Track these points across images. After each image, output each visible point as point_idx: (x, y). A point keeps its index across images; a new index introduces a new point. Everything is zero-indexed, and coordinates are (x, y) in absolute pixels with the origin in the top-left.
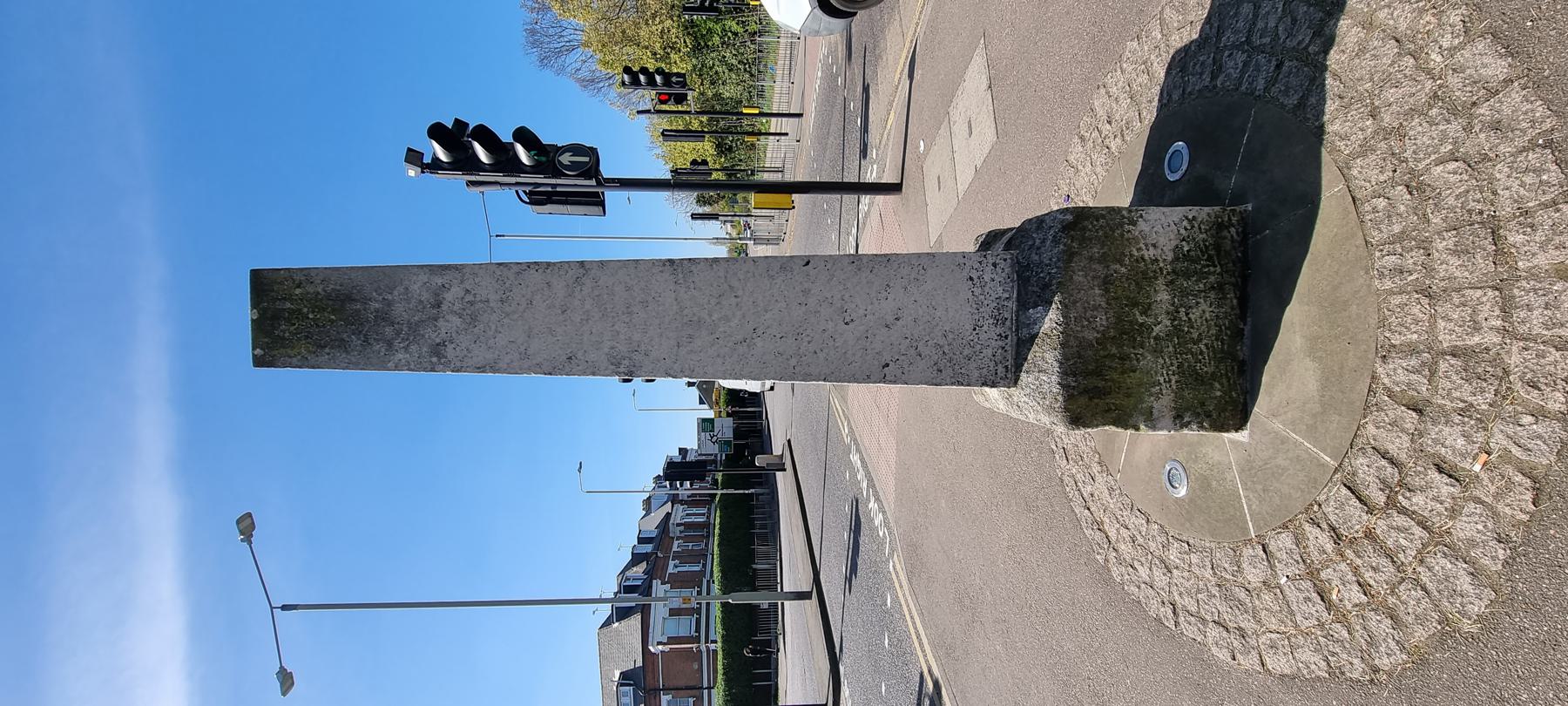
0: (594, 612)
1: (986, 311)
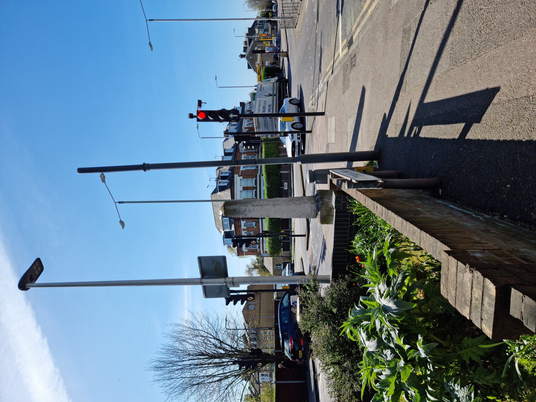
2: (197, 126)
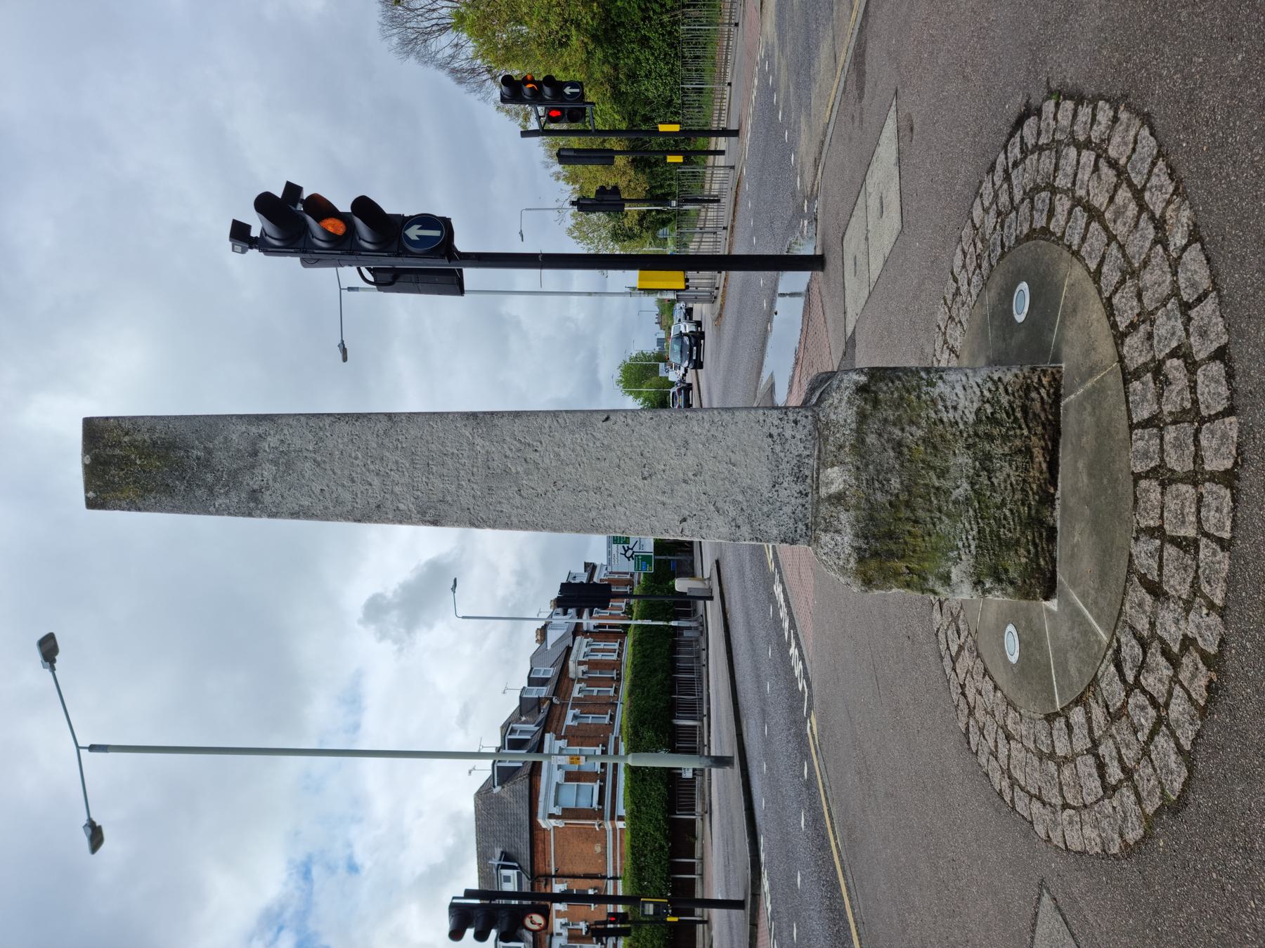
0: (470, 772)
1: (785, 467)
2: (452, 583)
